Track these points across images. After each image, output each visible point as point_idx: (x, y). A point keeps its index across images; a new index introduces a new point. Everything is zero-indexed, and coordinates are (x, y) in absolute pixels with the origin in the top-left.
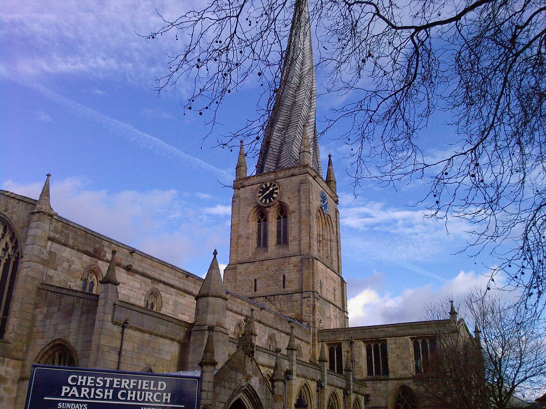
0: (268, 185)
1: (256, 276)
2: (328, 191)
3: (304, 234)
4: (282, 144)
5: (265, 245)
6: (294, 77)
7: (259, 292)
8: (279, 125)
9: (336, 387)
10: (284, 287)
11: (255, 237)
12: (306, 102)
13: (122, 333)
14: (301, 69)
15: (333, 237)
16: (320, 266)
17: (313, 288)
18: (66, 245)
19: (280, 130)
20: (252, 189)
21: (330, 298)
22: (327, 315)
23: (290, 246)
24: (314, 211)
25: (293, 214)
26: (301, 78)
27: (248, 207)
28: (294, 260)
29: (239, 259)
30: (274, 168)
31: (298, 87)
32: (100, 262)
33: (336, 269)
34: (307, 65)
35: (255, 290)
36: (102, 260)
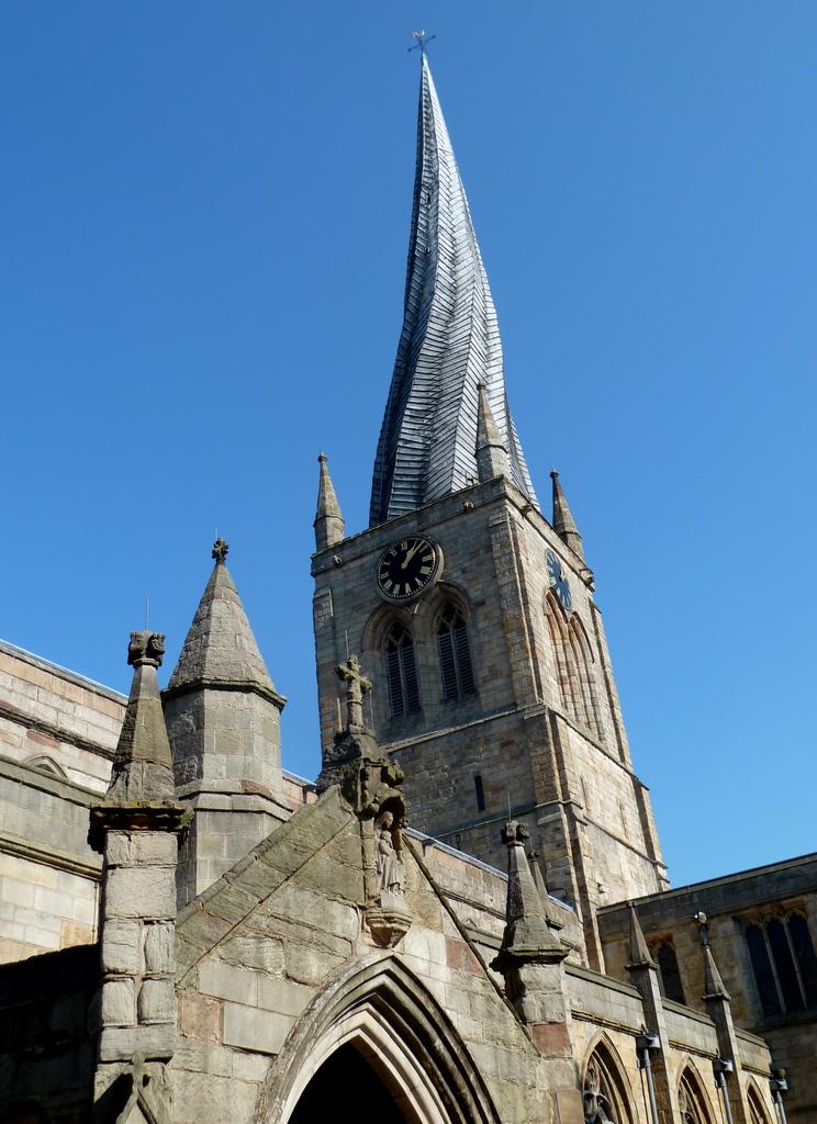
0: (404, 546)
2: (563, 550)
5: (415, 707)
8: (413, 405)
9: (693, 1051)
10: (482, 807)
14: (453, 273)
17: (566, 794)
20: (362, 566)
21: (615, 827)
23: (482, 695)
25: (481, 611)
26: (454, 290)
27: (356, 614)
31: (451, 313)
34: (465, 263)
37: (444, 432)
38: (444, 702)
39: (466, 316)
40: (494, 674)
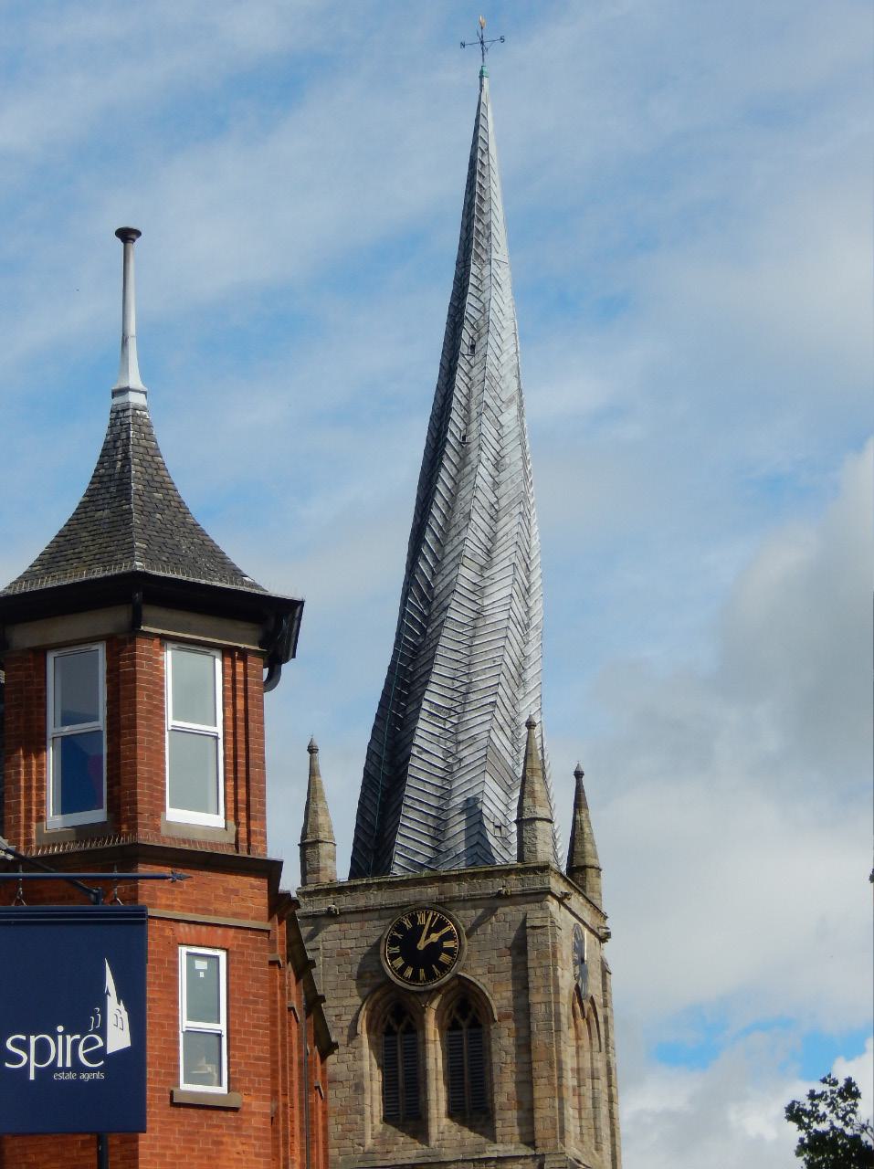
3: (541, 1091)
6: (474, 516)
8: (434, 695)
12: (518, 606)
14: (496, 485)
19: (438, 714)
23: (499, 1124)
24: (565, 1010)
31: (489, 552)
37: (471, 750)
39: (507, 563)
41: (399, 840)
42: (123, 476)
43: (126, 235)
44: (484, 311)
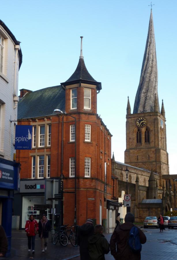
1: (138, 155)
4: (145, 100)
7: (139, 161)
8: (144, 91)
10: (149, 159)
11: (136, 139)
13: (140, 192)
14: (152, 63)
15: (164, 137)
16: (162, 151)
18: (118, 169)
19: (144, 93)
20: (134, 119)
22: (164, 168)
23: (151, 144)
28: (153, 149)
29: (130, 147)
30: (143, 110)
31: (151, 72)
32: (122, 171)
33: (165, 149)
34: (154, 61)
35: (138, 160)
36: (123, 170)
38: (144, 143)
40: (152, 142)
41: (139, 109)
42: (81, 67)
43: (82, 37)
44: (151, 40)
